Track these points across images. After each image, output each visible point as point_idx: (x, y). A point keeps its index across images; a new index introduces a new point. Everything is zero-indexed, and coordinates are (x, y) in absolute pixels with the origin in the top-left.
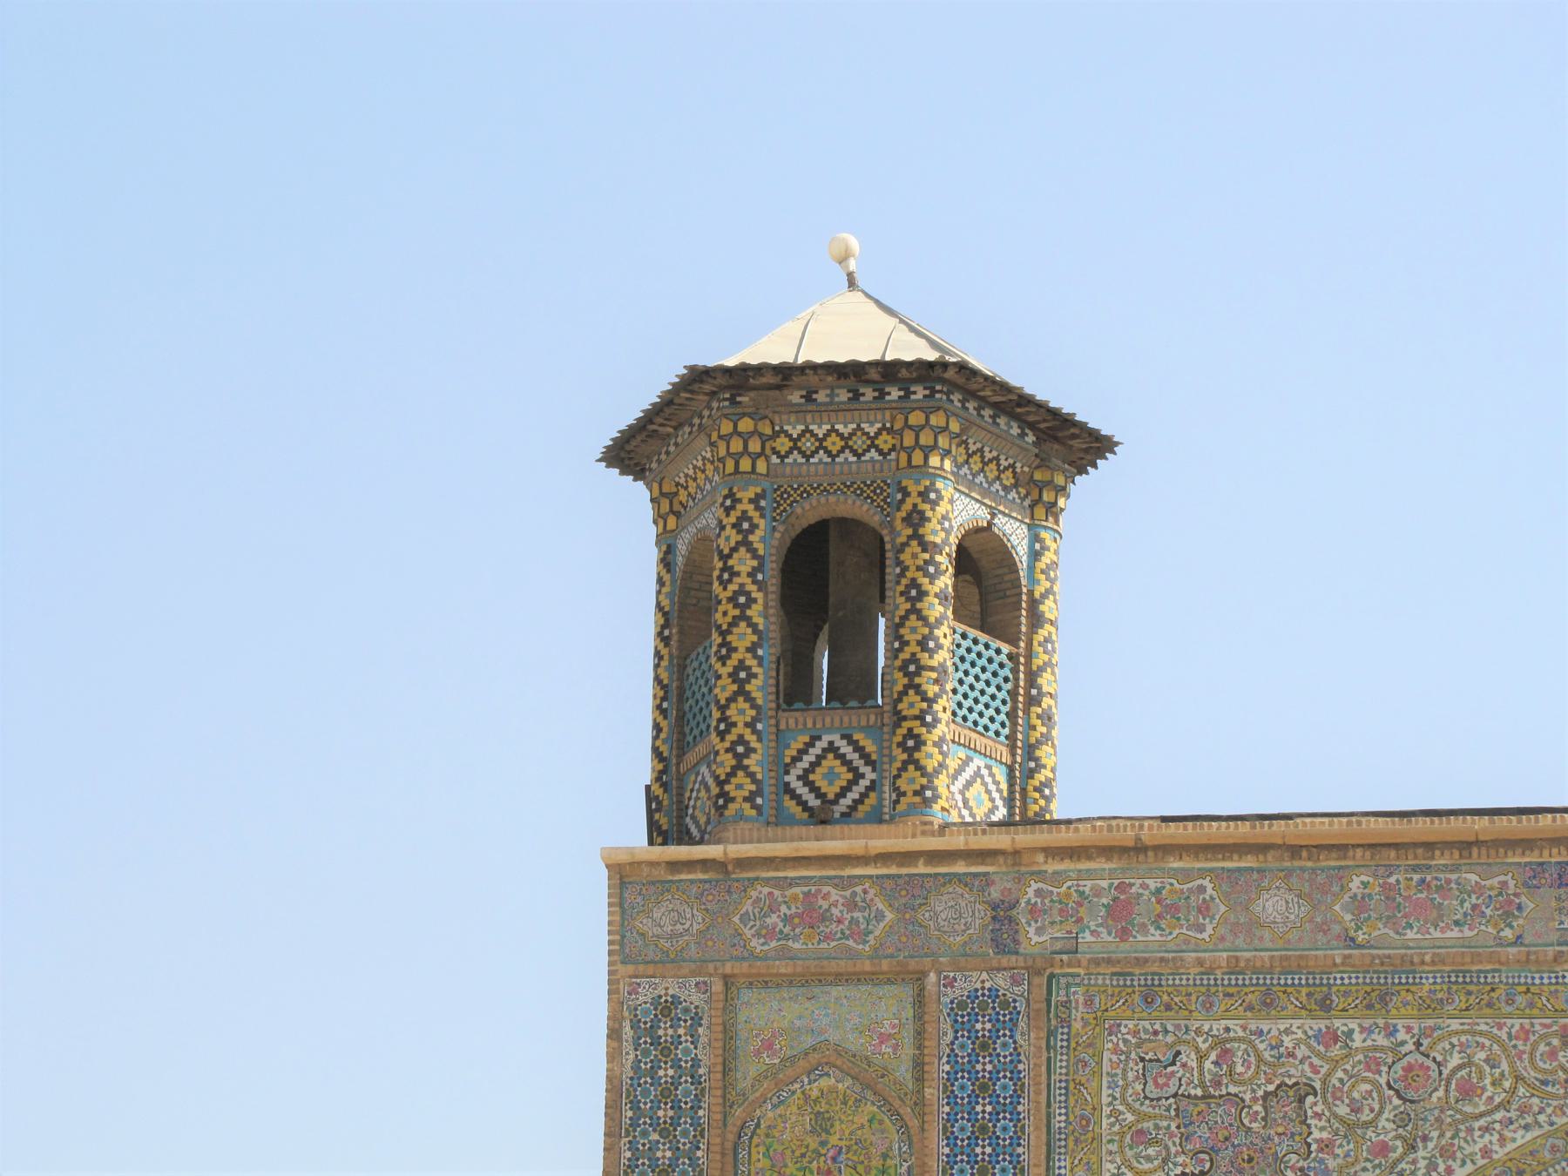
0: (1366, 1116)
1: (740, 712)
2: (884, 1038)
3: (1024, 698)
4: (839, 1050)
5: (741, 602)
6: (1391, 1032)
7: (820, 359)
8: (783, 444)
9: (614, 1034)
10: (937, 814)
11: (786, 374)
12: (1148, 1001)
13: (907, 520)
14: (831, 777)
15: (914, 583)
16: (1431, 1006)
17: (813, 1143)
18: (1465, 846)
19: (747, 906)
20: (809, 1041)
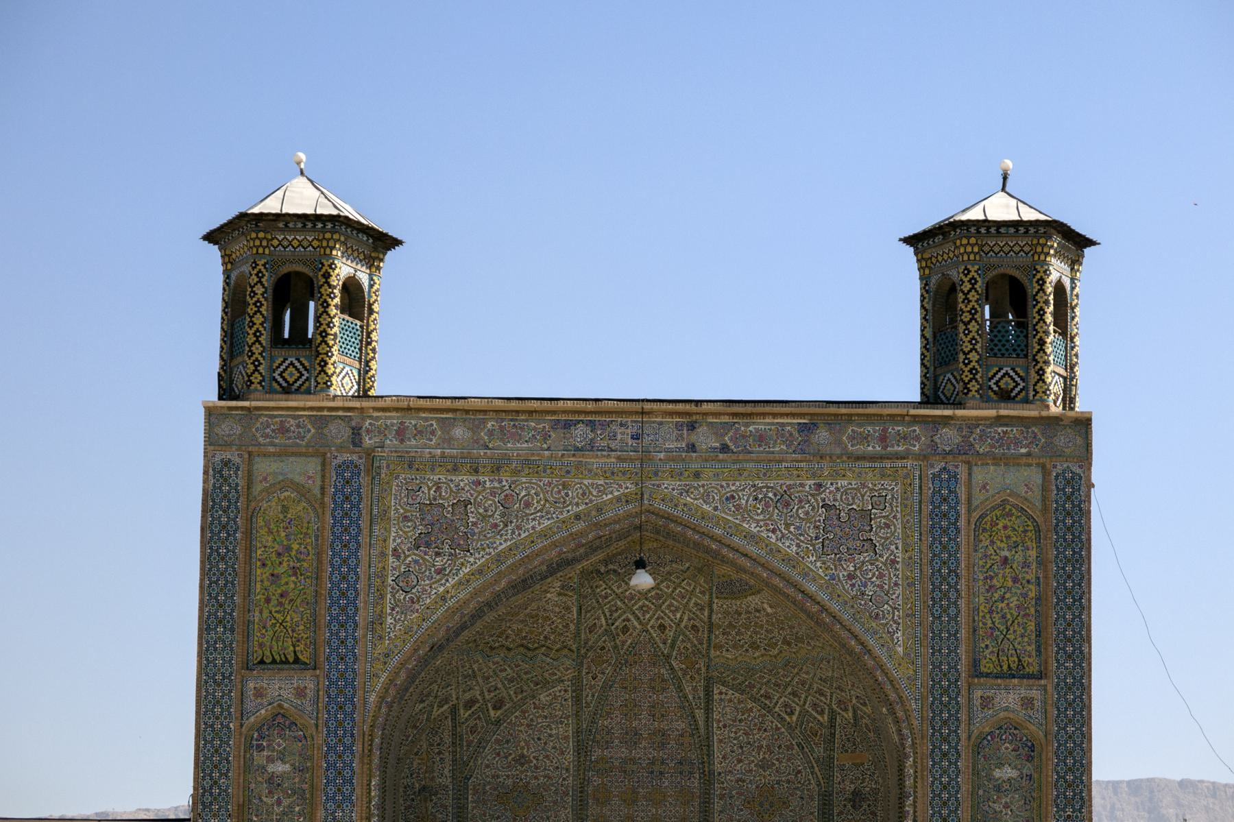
0: (490, 513)
1: (257, 349)
2: (309, 478)
3: (366, 341)
4: (292, 481)
5: (258, 305)
6: (500, 482)
7: (291, 212)
8: (275, 243)
9: (206, 472)
10: (332, 391)
11: (278, 217)
12: (410, 467)
13: (323, 276)
14: (291, 375)
15: (325, 301)
16: (516, 472)
17: (281, 516)
18: (531, 412)
19: (258, 425)
20: (281, 478)
